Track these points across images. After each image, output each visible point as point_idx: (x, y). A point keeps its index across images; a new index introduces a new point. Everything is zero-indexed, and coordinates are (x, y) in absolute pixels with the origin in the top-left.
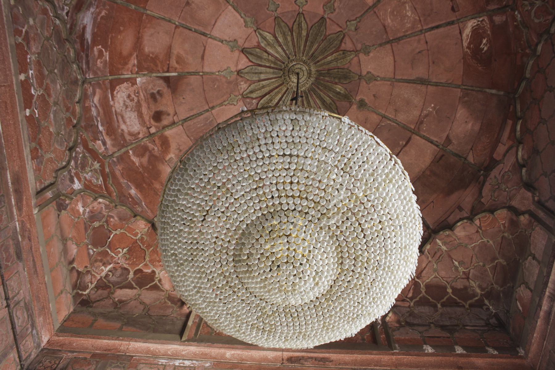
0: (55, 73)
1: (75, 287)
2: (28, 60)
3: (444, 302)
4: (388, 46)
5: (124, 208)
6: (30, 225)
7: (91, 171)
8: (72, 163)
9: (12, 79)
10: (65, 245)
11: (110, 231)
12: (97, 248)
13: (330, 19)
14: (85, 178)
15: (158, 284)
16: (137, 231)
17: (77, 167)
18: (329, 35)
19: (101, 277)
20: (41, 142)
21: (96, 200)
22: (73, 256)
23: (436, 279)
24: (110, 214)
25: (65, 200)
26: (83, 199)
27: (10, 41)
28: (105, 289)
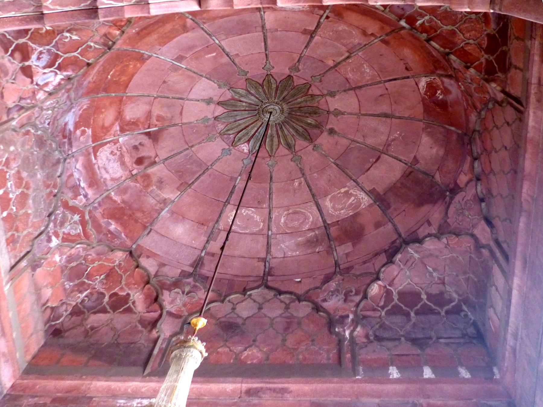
3: (418, 310)
23: (408, 286)
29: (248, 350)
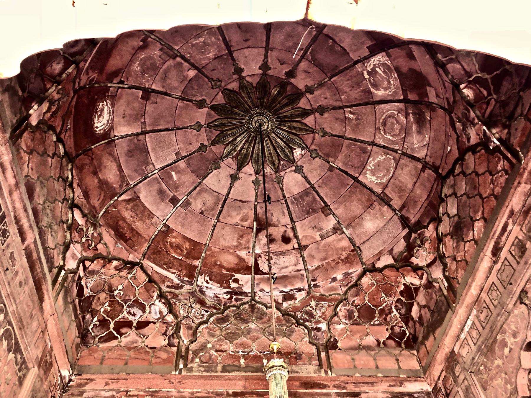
4: (235, 54)
11: (365, 304)
12: (375, 317)
13: (211, 103)
16: (370, 283)
17: (311, 322)
18: (225, 101)
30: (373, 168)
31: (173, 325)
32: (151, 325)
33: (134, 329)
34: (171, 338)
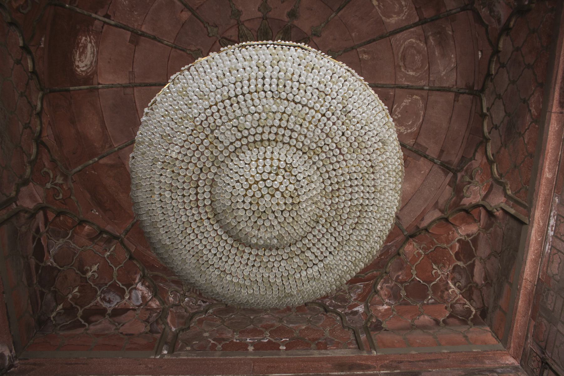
0: (254, 318)
1: (464, 322)
2: (238, 341)
5: (390, 264)
6: (386, 360)
7: (349, 293)
8: (339, 310)
9: (248, 359)
10: (418, 327)
11: (413, 280)
12: (428, 295)
14: (355, 300)
15: (471, 238)
16: (415, 253)
17: (344, 307)
19: (460, 294)
20: (313, 339)
21: (378, 291)
22: (432, 320)
24: (394, 279)
25: (372, 323)
26: (375, 304)
27: (217, 355)
28: (473, 292)
29: (531, 108)
30: (399, 116)
31: (158, 311)
32: (129, 313)
33: (107, 316)
34: (155, 325)
